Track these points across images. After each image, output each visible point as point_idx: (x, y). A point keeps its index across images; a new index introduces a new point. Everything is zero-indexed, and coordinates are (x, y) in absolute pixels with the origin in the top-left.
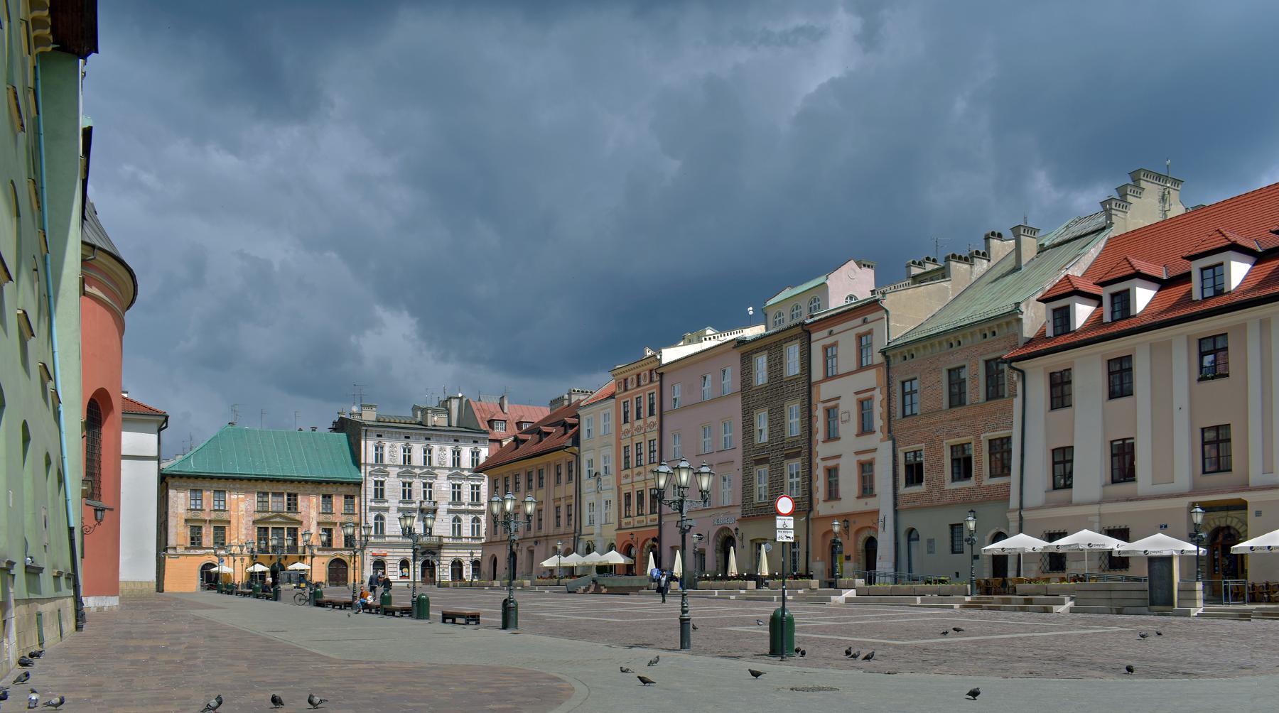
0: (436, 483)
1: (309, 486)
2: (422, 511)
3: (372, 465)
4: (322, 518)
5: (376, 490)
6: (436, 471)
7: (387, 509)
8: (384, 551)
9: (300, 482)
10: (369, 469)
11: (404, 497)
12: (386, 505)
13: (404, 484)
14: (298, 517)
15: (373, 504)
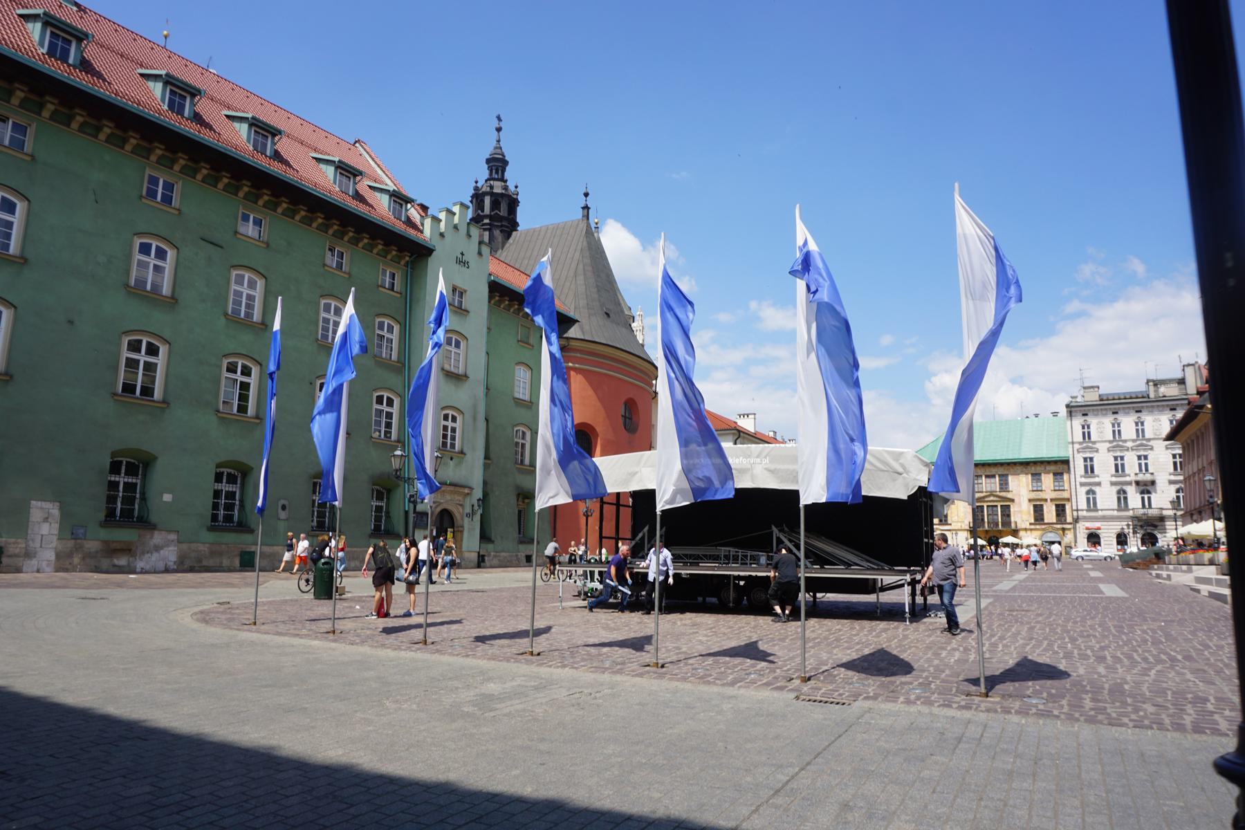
0: (1151, 455)
1: (1019, 468)
2: (1137, 483)
3: (1080, 443)
4: (1033, 495)
5: (1086, 467)
6: (1151, 443)
7: (1099, 484)
8: (1097, 525)
9: (1009, 464)
10: (1077, 446)
11: (1117, 470)
12: (1097, 480)
13: (1116, 458)
14: (1009, 495)
15: (1084, 480)
